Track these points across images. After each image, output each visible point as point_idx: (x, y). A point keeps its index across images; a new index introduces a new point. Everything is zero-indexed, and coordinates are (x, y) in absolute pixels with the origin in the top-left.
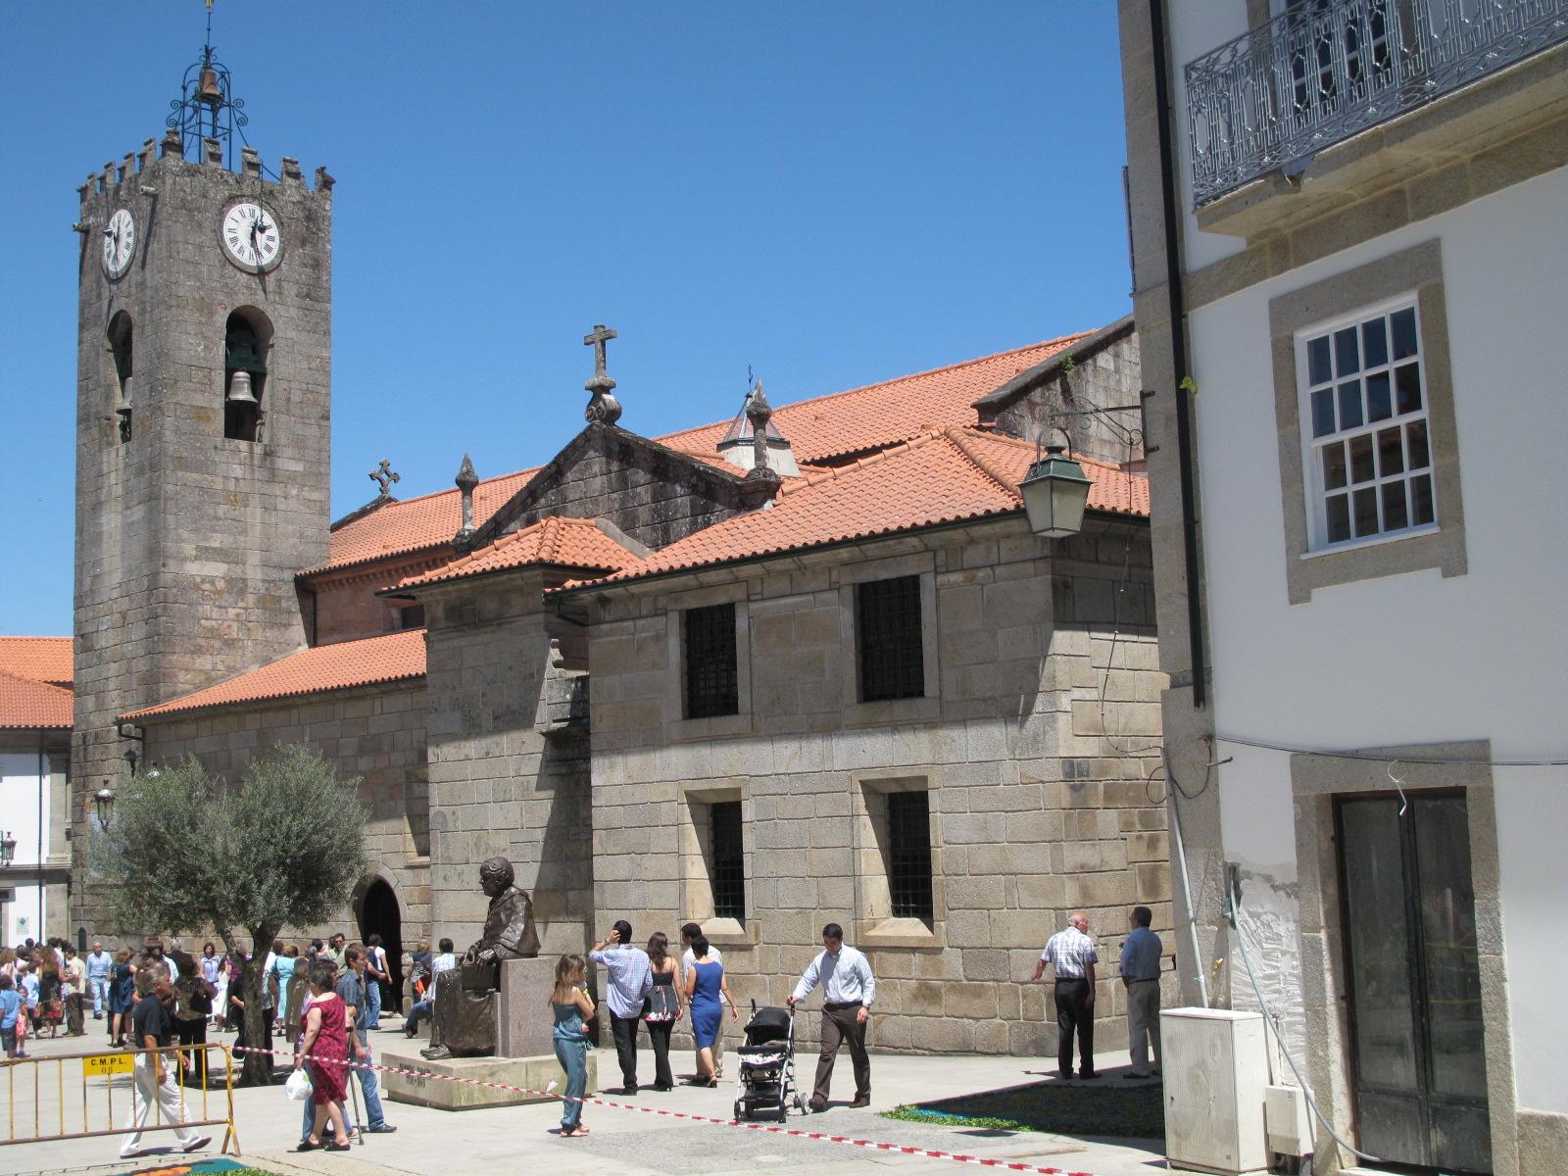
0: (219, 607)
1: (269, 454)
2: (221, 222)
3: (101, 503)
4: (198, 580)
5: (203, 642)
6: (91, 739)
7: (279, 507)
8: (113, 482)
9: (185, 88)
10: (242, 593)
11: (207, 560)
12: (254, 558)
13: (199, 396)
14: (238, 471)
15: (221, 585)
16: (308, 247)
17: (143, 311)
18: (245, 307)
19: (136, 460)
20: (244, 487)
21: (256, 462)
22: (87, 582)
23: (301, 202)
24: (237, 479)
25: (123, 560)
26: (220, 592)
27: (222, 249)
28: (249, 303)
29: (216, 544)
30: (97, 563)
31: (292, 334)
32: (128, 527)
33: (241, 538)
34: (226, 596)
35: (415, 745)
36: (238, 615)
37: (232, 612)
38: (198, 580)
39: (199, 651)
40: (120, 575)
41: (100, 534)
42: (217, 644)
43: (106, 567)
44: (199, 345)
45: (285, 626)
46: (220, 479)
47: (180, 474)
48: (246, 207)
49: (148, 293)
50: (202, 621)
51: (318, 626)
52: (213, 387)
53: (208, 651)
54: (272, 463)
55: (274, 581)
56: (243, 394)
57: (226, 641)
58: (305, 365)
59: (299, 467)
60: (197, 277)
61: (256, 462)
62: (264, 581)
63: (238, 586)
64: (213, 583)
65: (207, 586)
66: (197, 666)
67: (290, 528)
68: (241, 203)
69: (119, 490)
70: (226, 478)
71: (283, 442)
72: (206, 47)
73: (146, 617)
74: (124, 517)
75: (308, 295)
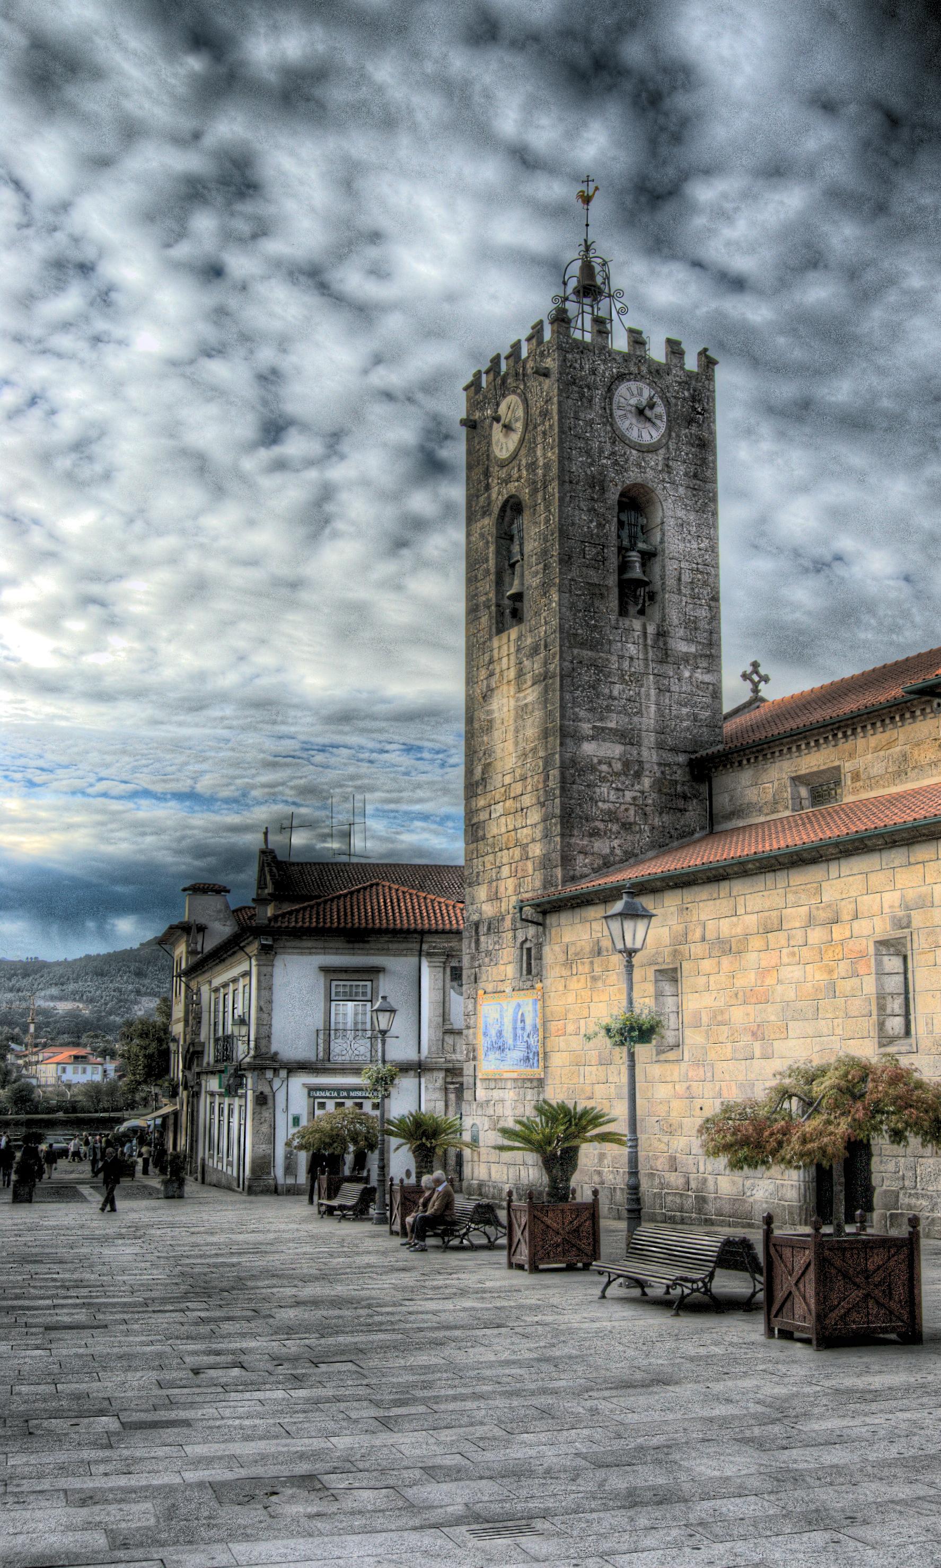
0: (617, 789)
1: (662, 634)
2: (611, 399)
3: (492, 690)
4: (595, 760)
5: (601, 826)
6: (483, 929)
7: (672, 689)
8: (505, 667)
9: (565, 284)
10: (638, 775)
11: (604, 741)
12: (650, 739)
13: (592, 572)
14: (632, 649)
15: (618, 766)
16: (694, 429)
17: (535, 491)
18: (635, 485)
19: (529, 641)
20: (638, 666)
21: (649, 642)
22: (478, 770)
23: (686, 383)
24: (631, 658)
25: (516, 744)
26: (617, 774)
27: (612, 425)
28: (639, 480)
29: (612, 725)
30: (488, 753)
31: (681, 513)
32: (522, 711)
33: (636, 719)
34: (623, 778)
35: (886, 910)
36: (634, 798)
37: (629, 795)
38: (595, 760)
39: (594, 833)
40: (514, 760)
41: (491, 721)
42: (615, 828)
43: (499, 753)
44: (591, 521)
45: (680, 810)
46: (614, 658)
47: (576, 651)
48: (633, 385)
49: (540, 472)
50: (600, 804)
51: (714, 812)
52: (606, 563)
53: (605, 833)
54: (665, 644)
55: (669, 765)
56: (636, 572)
57: (624, 825)
58: (695, 546)
59: (693, 649)
60: (588, 453)
61: (649, 642)
62: (659, 764)
63: (632, 769)
64: (610, 765)
65: (604, 768)
66: (596, 849)
67: (685, 711)
68: (629, 380)
69: (512, 674)
70: (621, 657)
71: (676, 622)
72: (586, 241)
73: (542, 800)
74: (518, 700)
75: (695, 476)
